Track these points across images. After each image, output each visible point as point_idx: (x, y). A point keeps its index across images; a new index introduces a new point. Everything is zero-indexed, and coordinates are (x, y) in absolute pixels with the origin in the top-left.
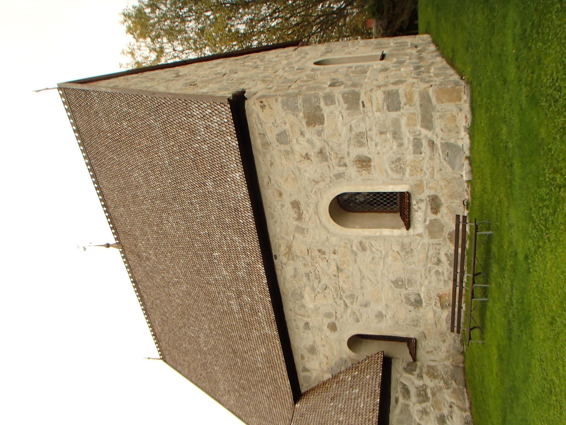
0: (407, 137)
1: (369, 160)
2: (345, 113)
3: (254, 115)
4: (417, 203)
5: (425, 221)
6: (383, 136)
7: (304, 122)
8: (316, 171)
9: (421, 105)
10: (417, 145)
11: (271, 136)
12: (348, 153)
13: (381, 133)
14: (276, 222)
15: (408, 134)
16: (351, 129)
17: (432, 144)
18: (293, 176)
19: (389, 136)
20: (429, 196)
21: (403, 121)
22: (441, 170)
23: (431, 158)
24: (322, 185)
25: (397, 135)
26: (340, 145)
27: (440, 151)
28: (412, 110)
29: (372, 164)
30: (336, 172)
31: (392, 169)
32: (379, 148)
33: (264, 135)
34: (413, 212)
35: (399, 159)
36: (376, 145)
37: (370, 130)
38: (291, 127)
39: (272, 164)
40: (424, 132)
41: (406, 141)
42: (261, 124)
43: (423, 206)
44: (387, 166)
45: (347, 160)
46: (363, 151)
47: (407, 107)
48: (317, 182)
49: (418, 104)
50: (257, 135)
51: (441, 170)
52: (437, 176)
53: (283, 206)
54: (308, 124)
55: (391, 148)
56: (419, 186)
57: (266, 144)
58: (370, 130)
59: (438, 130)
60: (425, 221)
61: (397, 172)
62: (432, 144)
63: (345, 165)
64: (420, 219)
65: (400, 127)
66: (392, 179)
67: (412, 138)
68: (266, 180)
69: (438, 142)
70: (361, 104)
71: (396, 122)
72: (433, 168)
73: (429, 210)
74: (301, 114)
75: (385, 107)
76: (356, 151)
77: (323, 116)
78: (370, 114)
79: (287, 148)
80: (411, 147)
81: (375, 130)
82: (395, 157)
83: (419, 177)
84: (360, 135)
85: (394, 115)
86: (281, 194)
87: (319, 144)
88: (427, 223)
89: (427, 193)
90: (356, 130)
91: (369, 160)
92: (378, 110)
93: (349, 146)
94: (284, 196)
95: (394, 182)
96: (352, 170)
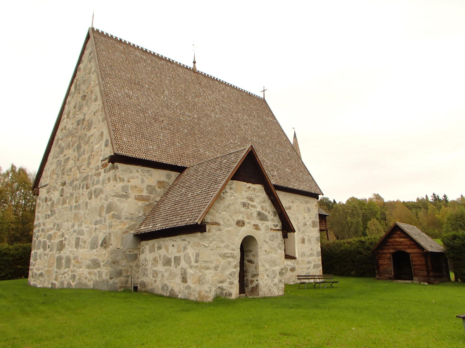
0: (311, 259)
1: (304, 243)
2: (315, 236)
3: (314, 201)
4: (293, 262)
5: (288, 265)
6: (310, 250)
7: (313, 220)
8: (301, 220)
9: (318, 264)
10: (309, 262)
11: (309, 205)
12: (305, 235)
13: (311, 249)
14: (284, 196)
15: (311, 259)
16: (312, 237)
17: (309, 268)
18: (299, 210)
19: (311, 252)
20: (295, 267)
21: (314, 257)
22: (302, 272)
23: (306, 268)
24: (297, 221)
25: (311, 255)
26: (308, 232)
27: (307, 271)
28: (317, 261)
29: (303, 244)
30: (300, 228)
31: (302, 252)
32: (307, 247)
33: (309, 203)
34: (291, 260)
35: (305, 255)
36: (308, 247)
37: (312, 245)
38: (312, 215)
39: (301, 202)
40: (312, 265)
41: (310, 258)
42: (312, 203)
43: (292, 265)
44: (302, 250)
45: (304, 234)
46: (306, 241)
47: (318, 259)
48: (297, 219)
49: (318, 263)
50: (309, 200)
51: (302, 272)
52: (301, 270)
53: (289, 202)
54: (313, 221)
55: (308, 252)
56: (298, 263)
57: (307, 202)
58: (312, 245)
59: (313, 270)
60: (288, 265)
61: (302, 254)
62: (309, 268)
63: (303, 233)
64: (288, 263)
65: (313, 256)
66: (299, 252)
67: (310, 260)
68: (297, 198)
69: (309, 271)
70: (318, 242)
71: (314, 255)
72: (303, 269)
73: (291, 267)
74: (315, 220)
75: (318, 251)
76: (306, 238)
77: (314, 228)
78: (315, 245)
79: (306, 211)
80: (308, 260)
81: (312, 247)
82: (305, 254)
83: (301, 263)
84: (311, 241)
85: (316, 254)
86: (293, 202)
87: (308, 223)
88: (287, 266)
89: (296, 266)
90: (312, 239)
91: (304, 243)
92: (317, 249)
93: (307, 236)
94: (292, 203)
95: (299, 252)
96: (301, 236)
